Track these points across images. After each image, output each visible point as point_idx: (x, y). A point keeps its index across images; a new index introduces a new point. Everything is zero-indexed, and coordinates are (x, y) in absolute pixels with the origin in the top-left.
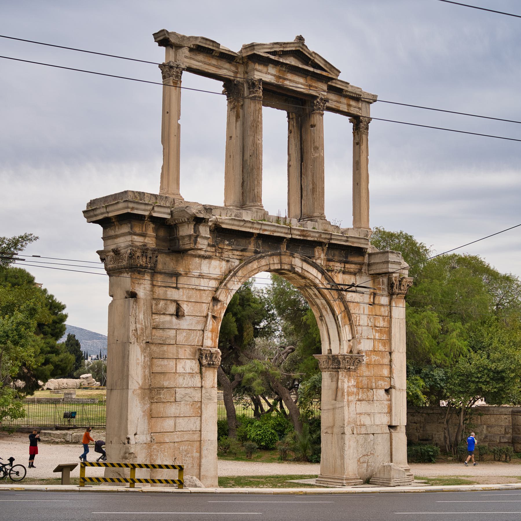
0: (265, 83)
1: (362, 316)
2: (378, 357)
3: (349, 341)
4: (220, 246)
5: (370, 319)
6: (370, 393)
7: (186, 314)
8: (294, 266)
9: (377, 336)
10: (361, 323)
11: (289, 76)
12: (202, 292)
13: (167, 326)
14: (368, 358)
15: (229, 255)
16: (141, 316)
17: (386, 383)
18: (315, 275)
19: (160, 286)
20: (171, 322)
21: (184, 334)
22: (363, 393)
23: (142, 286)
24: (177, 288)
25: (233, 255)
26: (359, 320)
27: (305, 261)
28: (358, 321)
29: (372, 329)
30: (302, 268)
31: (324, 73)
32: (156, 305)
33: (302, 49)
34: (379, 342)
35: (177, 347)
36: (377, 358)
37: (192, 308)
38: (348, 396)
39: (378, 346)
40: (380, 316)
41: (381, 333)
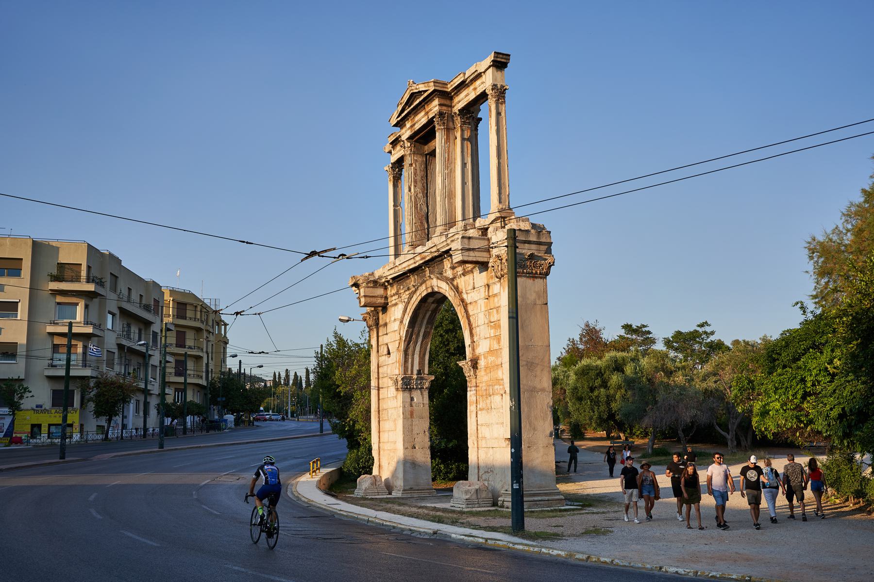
6: (488, 401)
9: (492, 332)
11: (417, 118)
14: (485, 360)
17: (501, 387)
22: (483, 401)
24: (387, 334)
27: (438, 278)
29: (488, 326)
31: (426, 94)
33: (412, 90)
34: (494, 339)
38: (470, 406)
39: (493, 344)
40: (495, 308)
41: (495, 329)
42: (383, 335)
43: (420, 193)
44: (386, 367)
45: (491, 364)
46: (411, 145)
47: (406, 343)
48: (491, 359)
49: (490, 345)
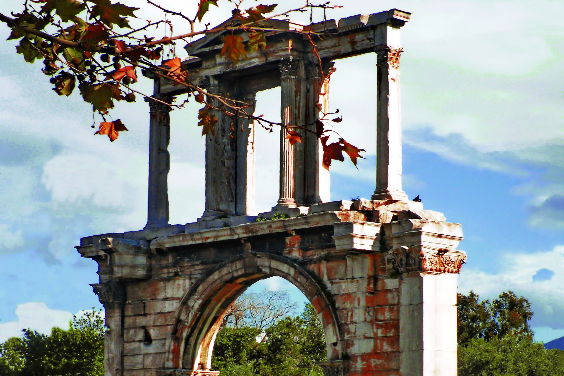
0: (216, 77)
1: (356, 311)
2: (381, 361)
3: (335, 344)
4: (181, 265)
5: (368, 312)
7: (153, 338)
8: (260, 267)
10: (354, 319)
12: (167, 315)
13: (137, 352)
14: (365, 363)
15: (191, 272)
16: (113, 346)
18: (286, 271)
19: (131, 316)
20: (139, 348)
21: (151, 358)
23: (113, 319)
24: (145, 315)
25: (195, 270)
26: (352, 316)
28: (349, 318)
29: (372, 325)
30: (270, 267)
32: (127, 334)
35: (144, 371)
36: (379, 362)
37: (158, 332)
39: (382, 346)
41: (386, 328)
42: (135, 316)
43: (228, 145)
44: (141, 357)
45: (375, 366)
46: (219, 83)
47: (189, 330)
48: (374, 362)
49: (376, 346)
